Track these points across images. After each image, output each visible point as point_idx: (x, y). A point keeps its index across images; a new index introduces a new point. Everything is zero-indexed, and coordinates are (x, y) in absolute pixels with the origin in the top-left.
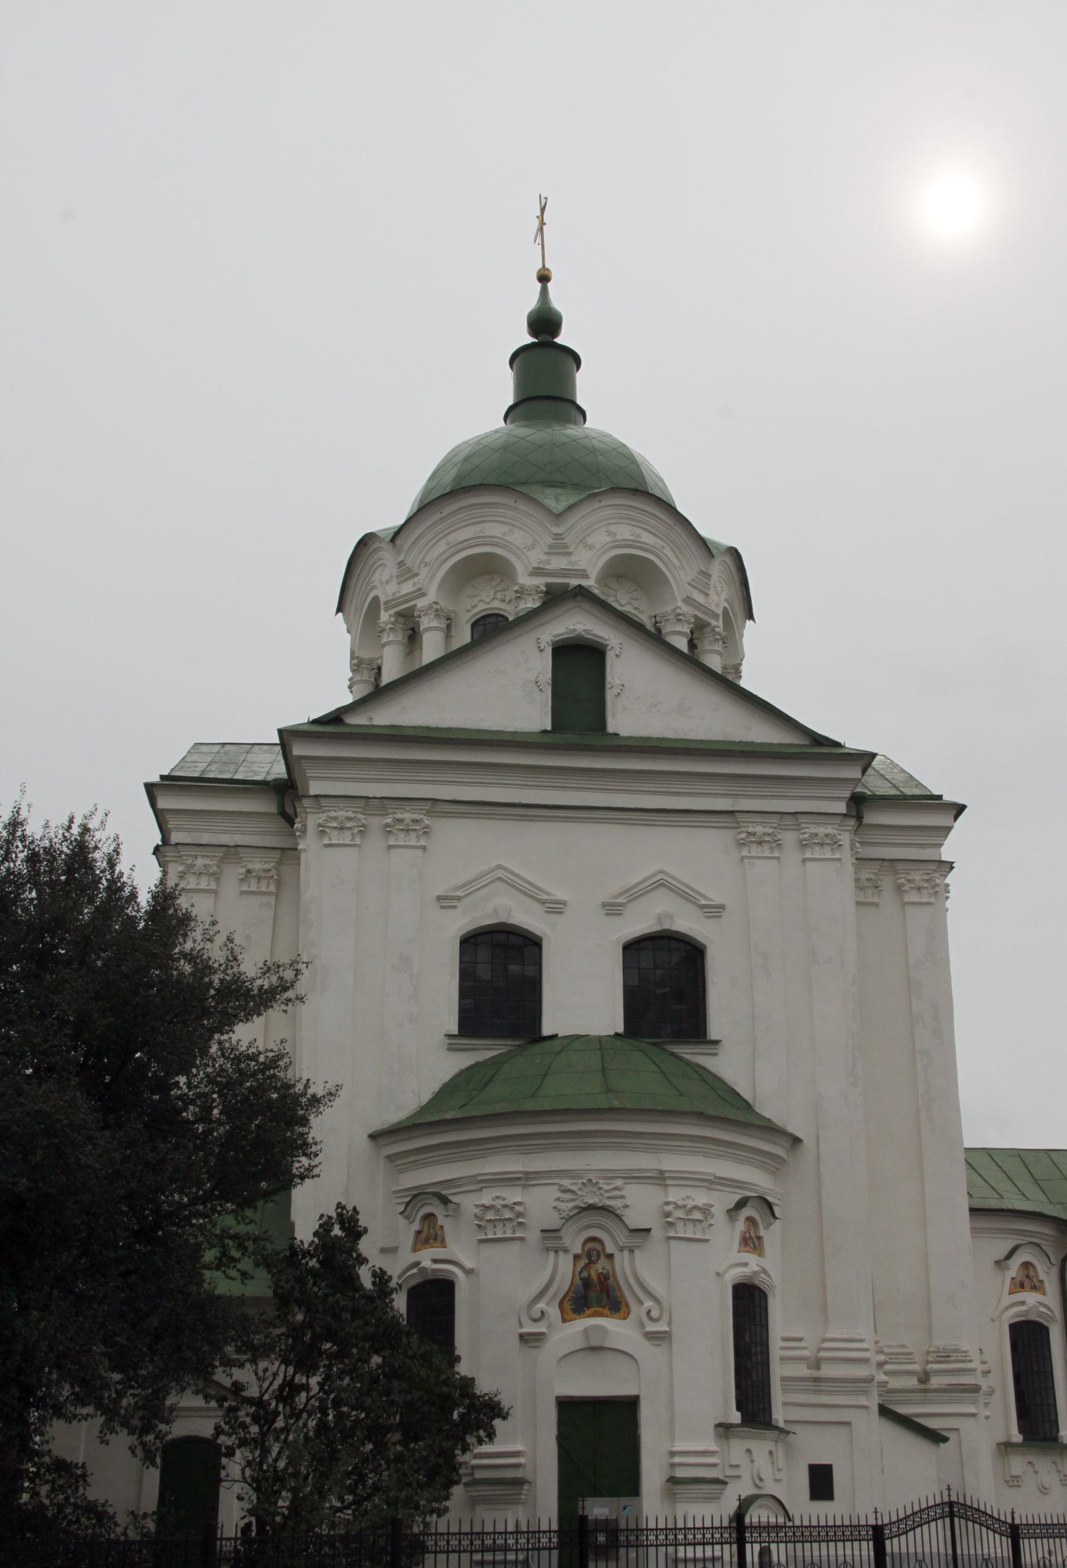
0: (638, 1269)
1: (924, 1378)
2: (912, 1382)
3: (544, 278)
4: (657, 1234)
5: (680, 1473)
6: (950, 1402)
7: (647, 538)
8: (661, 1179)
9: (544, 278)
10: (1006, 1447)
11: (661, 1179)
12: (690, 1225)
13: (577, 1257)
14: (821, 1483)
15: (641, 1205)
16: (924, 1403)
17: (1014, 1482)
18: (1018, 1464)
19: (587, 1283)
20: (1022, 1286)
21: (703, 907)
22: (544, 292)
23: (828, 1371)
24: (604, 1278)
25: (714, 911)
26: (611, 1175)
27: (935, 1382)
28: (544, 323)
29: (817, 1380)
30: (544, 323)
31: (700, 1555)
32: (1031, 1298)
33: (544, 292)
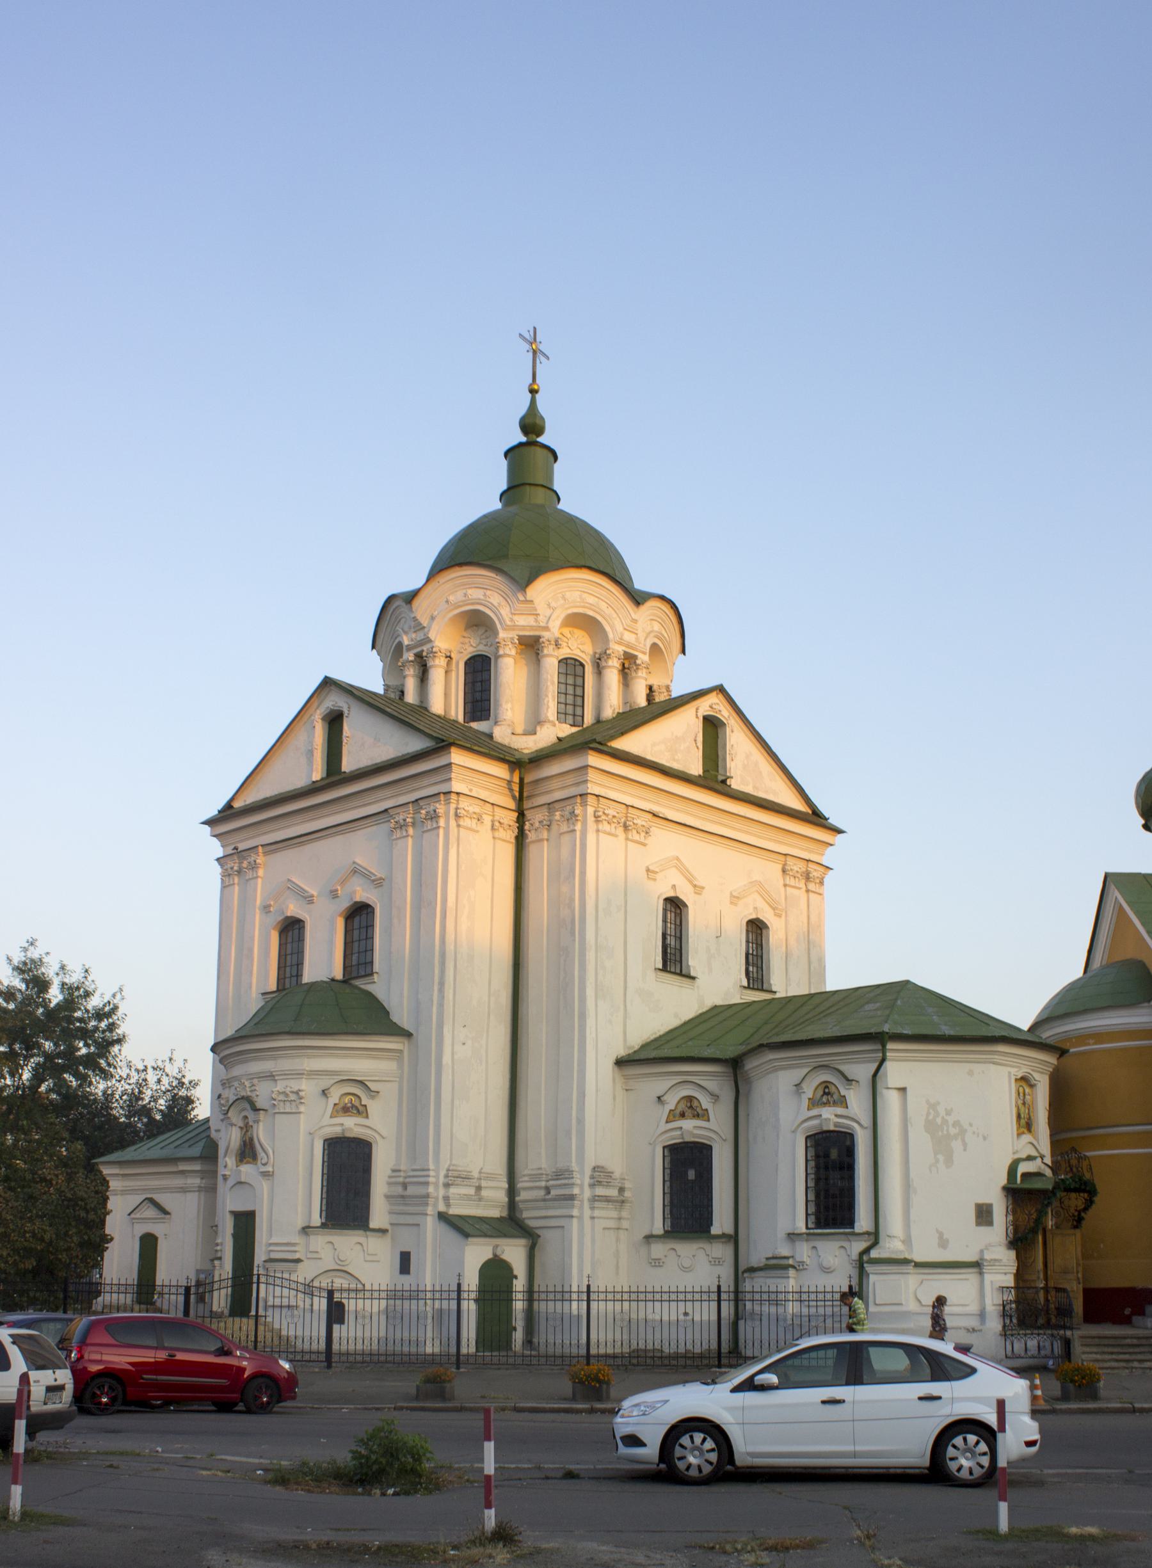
0: (261, 1133)
1: (548, 1190)
2: (542, 1193)
3: (533, 392)
4: (271, 1111)
5: (274, 1256)
6: (554, 1208)
7: (475, 594)
8: (271, 1077)
9: (533, 392)
10: (649, 1238)
11: (271, 1077)
12: (288, 1104)
13: (241, 1128)
14: (405, 1263)
15: (263, 1093)
16: (547, 1208)
17: (657, 1263)
18: (659, 1249)
19: (245, 1142)
20: (683, 1115)
21: (374, 881)
22: (533, 402)
23: (411, 1190)
24: (251, 1139)
25: (378, 883)
26: (251, 1077)
27: (553, 1192)
28: (532, 425)
29: (403, 1197)
30: (532, 425)
31: (115, 1296)
32: (688, 1124)
33: (533, 402)
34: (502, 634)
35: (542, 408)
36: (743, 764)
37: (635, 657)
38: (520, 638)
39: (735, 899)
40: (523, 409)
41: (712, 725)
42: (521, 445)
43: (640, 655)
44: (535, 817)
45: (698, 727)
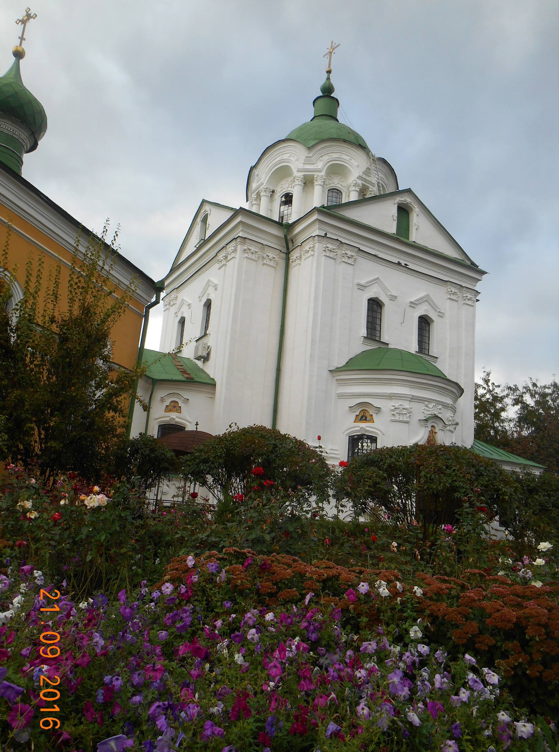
3: (329, 72)
9: (329, 72)
22: (328, 79)
28: (328, 90)
33: (328, 79)
34: (296, 174)
35: (333, 81)
36: (421, 232)
37: (368, 188)
38: (304, 175)
39: (413, 305)
40: (322, 81)
41: (404, 211)
42: (320, 97)
43: (370, 186)
44: (294, 255)
45: (394, 211)
